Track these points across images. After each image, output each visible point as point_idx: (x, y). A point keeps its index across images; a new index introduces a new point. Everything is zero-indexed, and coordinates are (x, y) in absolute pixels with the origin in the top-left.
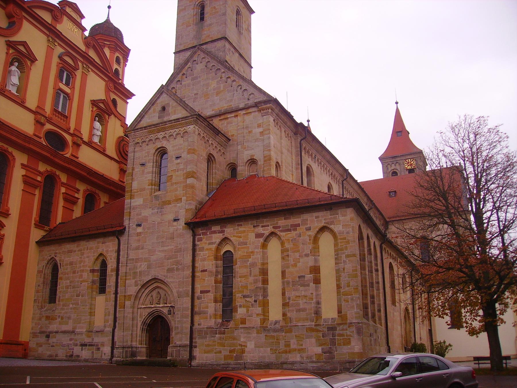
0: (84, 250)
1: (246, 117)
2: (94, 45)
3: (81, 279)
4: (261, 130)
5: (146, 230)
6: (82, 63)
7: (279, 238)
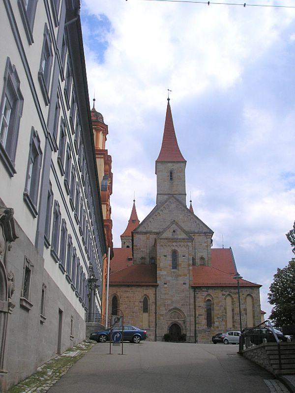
7: (231, 296)
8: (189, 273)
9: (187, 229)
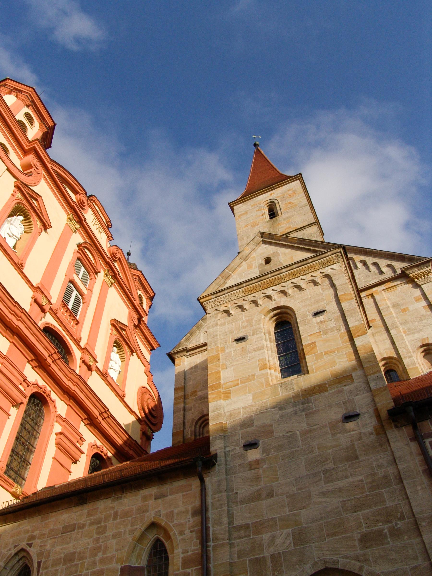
0: (106, 519)
2: (119, 258)
5: (273, 453)
6: (105, 271)
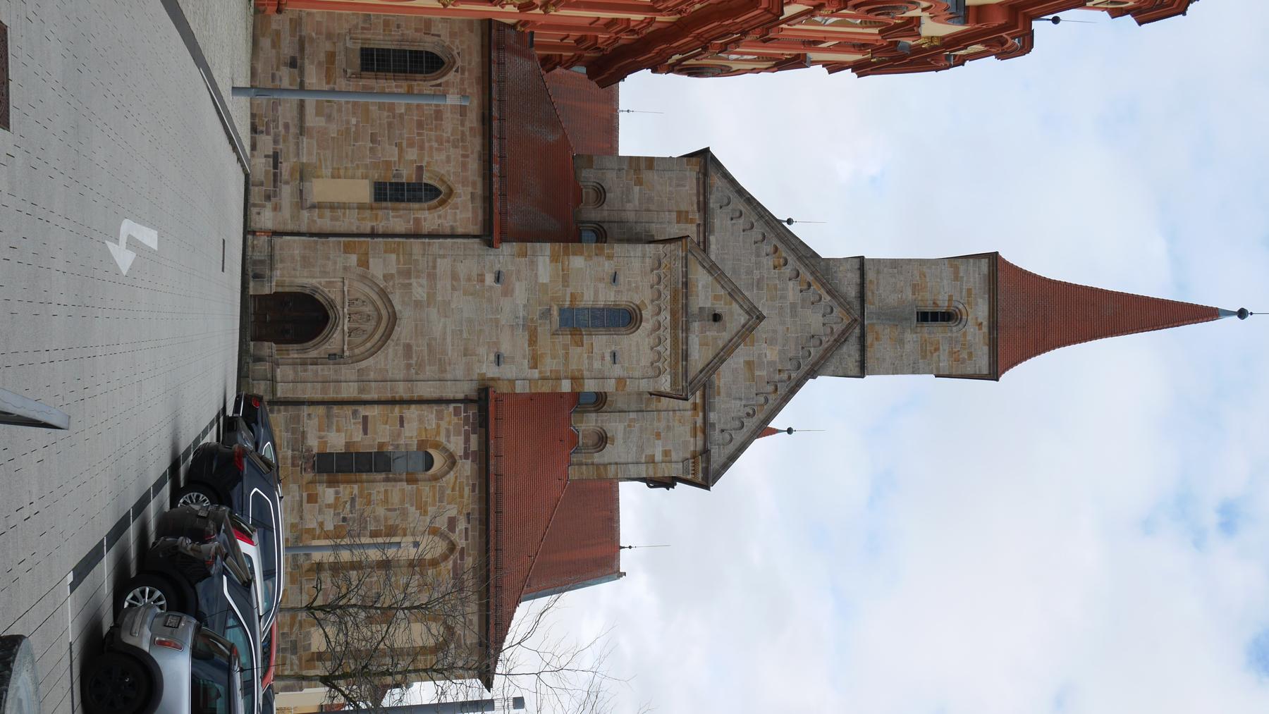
0: (464, 148)
1: (688, 428)
3: (404, 145)
4: (659, 457)
7: (445, 557)
8: (544, 379)
9: (724, 377)
